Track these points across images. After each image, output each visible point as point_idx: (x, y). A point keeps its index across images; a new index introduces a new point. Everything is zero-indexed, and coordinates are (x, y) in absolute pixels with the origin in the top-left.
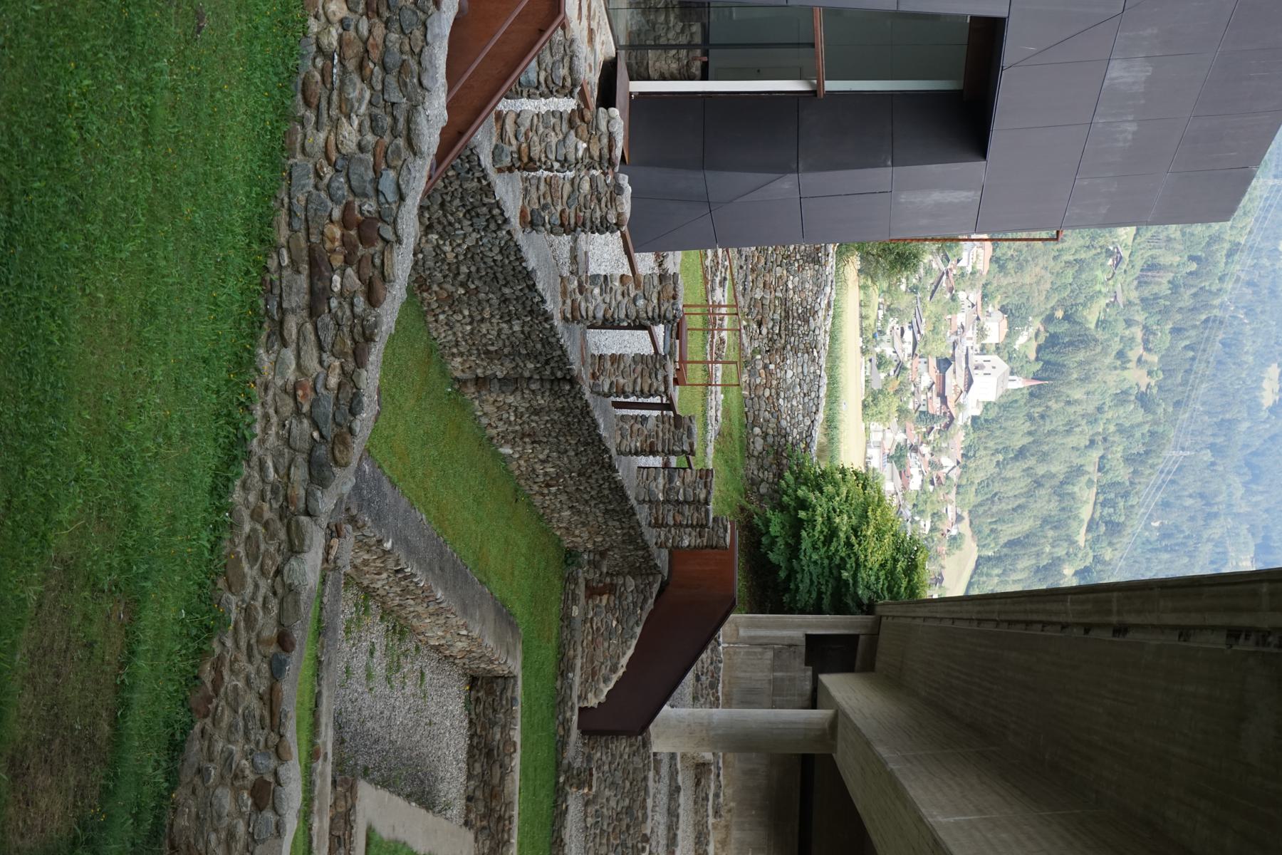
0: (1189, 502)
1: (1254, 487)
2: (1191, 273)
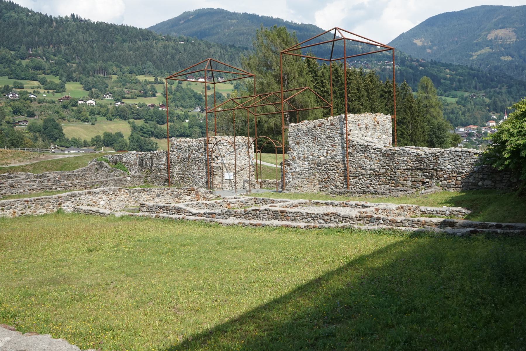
2: (477, 78)
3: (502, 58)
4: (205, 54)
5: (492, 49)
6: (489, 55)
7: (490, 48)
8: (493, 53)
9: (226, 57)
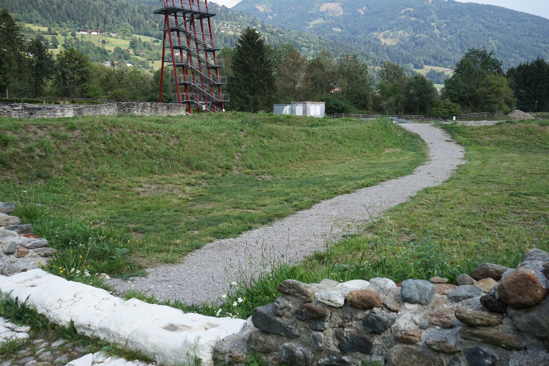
0: (367, 46)
1: (359, 33)
3: (334, 29)
4: (92, 7)
5: (325, 20)
6: (323, 26)
7: (323, 19)
8: (326, 24)
9: (113, 12)
